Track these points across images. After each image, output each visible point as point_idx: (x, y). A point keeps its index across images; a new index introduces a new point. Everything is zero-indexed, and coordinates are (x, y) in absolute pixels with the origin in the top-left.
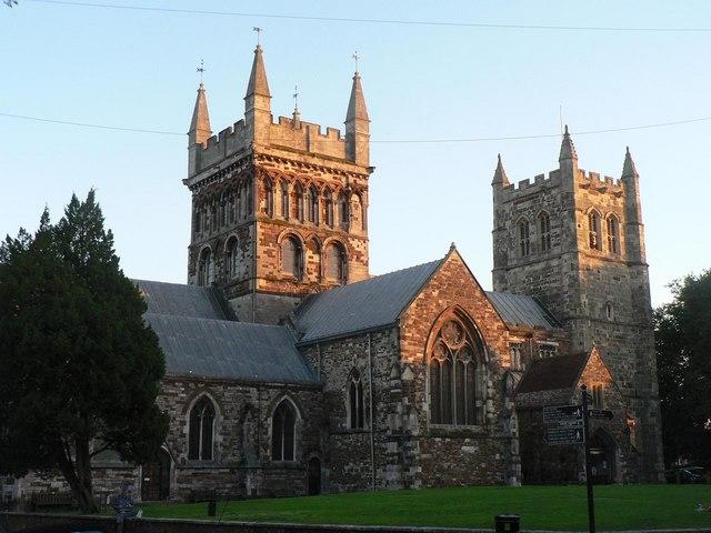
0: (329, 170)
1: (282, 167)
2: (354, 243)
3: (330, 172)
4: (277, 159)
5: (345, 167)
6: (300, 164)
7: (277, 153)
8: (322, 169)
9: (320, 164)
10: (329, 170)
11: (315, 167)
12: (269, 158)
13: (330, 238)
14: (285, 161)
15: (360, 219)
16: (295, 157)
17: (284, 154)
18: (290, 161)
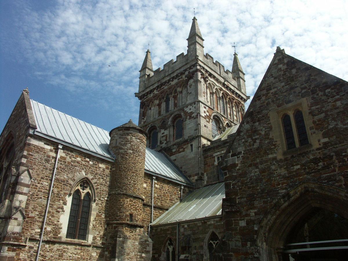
0: (173, 78)
1: (152, 95)
2: (187, 110)
3: (176, 79)
4: (147, 93)
5: (182, 70)
6: (158, 87)
7: (148, 90)
8: (169, 80)
9: (168, 78)
10: (173, 78)
11: (165, 82)
12: (144, 95)
13: (173, 116)
14: (151, 91)
15: (193, 92)
16: (156, 85)
17: (152, 88)
18: (154, 89)
